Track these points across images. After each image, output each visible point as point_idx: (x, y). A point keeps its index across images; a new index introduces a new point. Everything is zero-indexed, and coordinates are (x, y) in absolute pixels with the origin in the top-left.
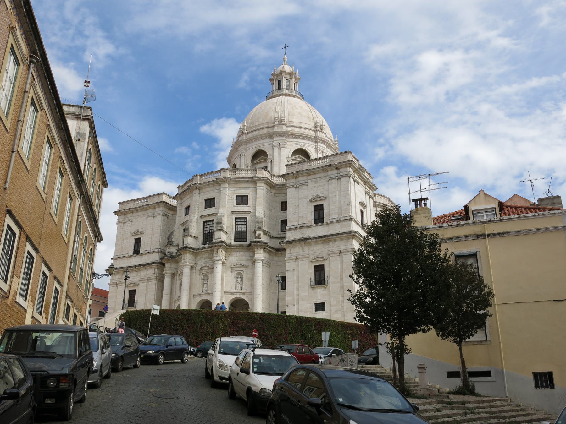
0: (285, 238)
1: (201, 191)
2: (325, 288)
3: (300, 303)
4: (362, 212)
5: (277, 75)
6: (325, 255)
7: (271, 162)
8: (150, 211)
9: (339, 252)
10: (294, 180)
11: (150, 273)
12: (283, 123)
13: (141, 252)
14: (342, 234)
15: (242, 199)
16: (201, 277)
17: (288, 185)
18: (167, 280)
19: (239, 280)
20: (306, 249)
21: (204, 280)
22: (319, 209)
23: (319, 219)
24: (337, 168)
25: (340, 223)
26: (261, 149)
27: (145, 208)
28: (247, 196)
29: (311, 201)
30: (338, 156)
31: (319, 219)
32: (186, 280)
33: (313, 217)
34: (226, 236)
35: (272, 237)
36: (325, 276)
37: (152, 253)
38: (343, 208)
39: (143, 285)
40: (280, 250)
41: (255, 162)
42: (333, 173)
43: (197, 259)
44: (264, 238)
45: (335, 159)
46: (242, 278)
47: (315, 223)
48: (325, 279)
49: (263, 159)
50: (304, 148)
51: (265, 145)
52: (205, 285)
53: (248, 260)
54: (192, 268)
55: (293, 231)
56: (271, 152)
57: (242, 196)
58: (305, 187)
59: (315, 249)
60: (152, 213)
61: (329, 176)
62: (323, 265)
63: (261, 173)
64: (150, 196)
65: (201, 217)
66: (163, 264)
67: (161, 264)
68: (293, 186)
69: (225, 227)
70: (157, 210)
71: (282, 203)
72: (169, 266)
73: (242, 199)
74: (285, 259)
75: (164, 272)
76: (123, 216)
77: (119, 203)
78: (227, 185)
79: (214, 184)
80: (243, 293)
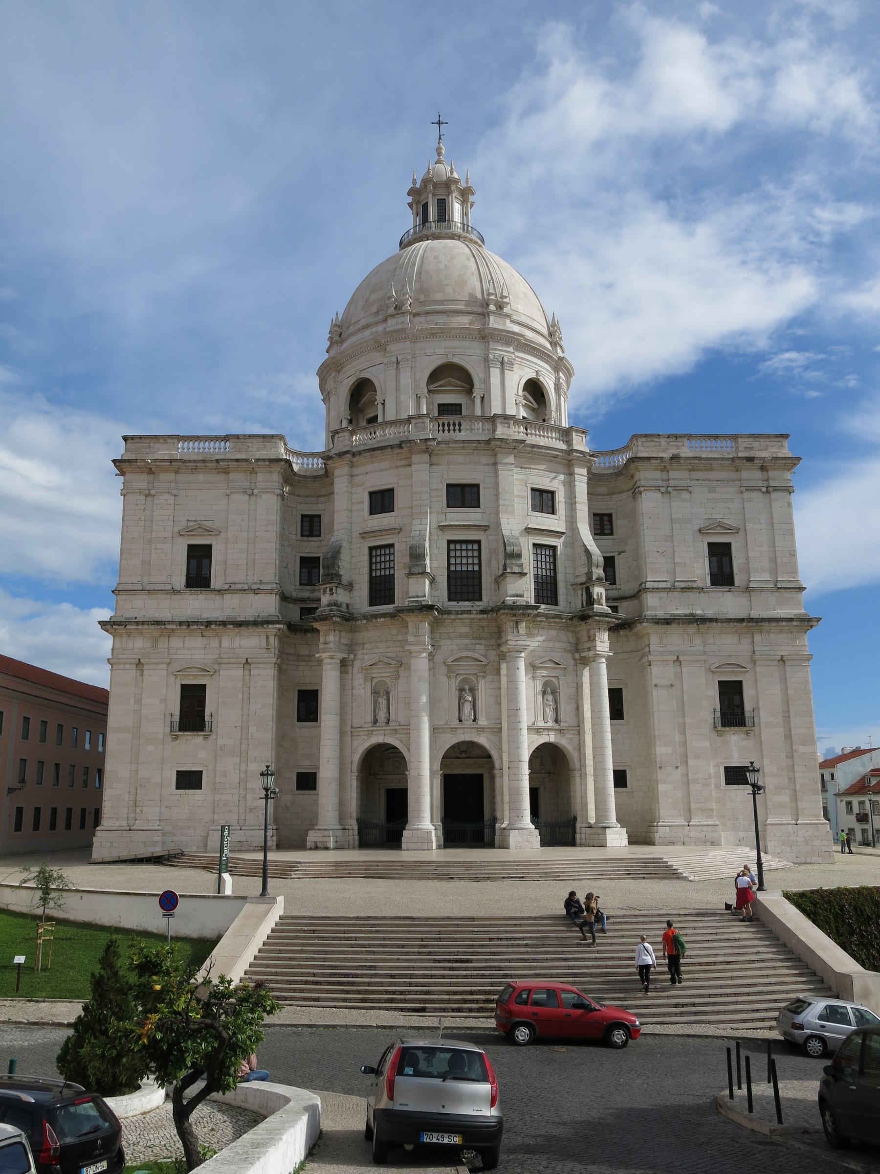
1: (434, 459)
3: (691, 762)
5: (435, 186)
7: (483, 398)
8: (238, 478)
9: (779, 658)
10: (658, 474)
12: (505, 310)
13: (216, 581)
14: (791, 620)
15: (544, 500)
16: (455, 684)
19: (550, 697)
20: (698, 640)
21: (461, 690)
23: (722, 574)
24: (763, 468)
25: (776, 594)
26: (456, 360)
27: (221, 466)
28: (552, 493)
30: (762, 440)
31: (722, 574)
33: (708, 571)
36: (748, 706)
37: (256, 592)
38: (779, 560)
41: (432, 387)
42: (752, 476)
43: (437, 636)
45: (756, 445)
46: (554, 692)
47: (713, 583)
48: (748, 714)
49: (450, 384)
50: (541, 379)
51: (468, 356)
52: (467, 708)
53: (566, 651)
55: (664, 595)
56: (482, 375)
57: (541, 492)
58: (685, 495)
60: (247, 484)
61: (745, 483)
62: (740, 682)
64: (237, 437)
68: (657, 488)
70: (260, 477)
72: (337, 639)
76: (145, 476)
77: (125, 438)
78: (511, 459)
79: (476, 449)
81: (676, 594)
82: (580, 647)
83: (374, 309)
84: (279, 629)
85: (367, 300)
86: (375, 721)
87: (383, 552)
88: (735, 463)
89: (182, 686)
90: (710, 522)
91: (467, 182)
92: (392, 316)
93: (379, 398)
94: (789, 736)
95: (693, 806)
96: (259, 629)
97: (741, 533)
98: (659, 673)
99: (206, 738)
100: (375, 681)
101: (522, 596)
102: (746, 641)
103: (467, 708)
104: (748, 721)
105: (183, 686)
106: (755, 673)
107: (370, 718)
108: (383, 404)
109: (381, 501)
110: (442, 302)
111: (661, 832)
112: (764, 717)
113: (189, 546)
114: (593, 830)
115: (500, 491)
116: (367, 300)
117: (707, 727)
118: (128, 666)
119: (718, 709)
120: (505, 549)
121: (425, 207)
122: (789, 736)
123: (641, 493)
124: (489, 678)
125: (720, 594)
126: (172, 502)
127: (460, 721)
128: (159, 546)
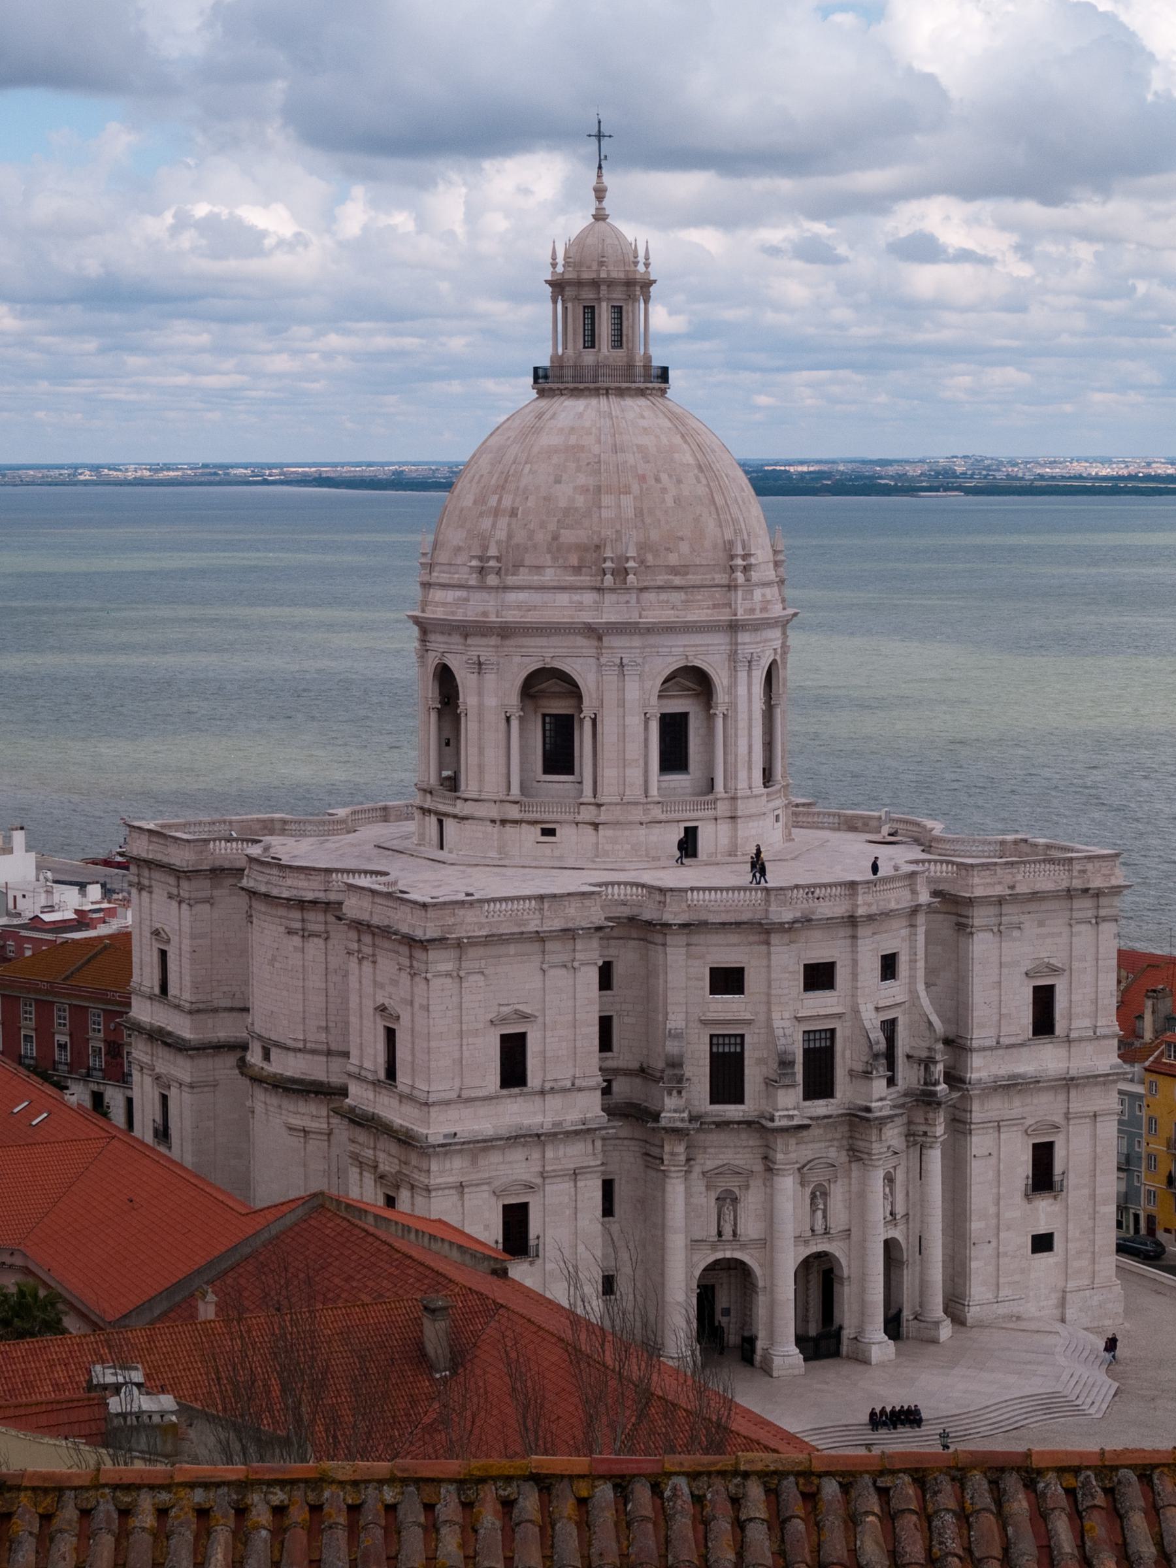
2: (1055, 1198)
6: (1058, 1119)
15: (889, 966)
16: (808, 1191)
21: (813, 1197)
22: (1044, 999)
23: (1043, 1023)
26: (697, 663)
33: (1031, 1020)
36: (1058, 1168)
37: (580, 1090)
39: (558, 1192)
42: (1084, 906)
47: (1034, 1034)
48: (1057, 1178)
55: (988, 1053)
56: (725, 682)
58: (1016, 933)
59: (1035, 1101)
64: (554, 896)
76: (453, 953)
81: (1000, 1052)
82: (913, 1127)
83: (574, 560)
85: (555, 538)
86: (720, 1234)
87: (727, 1041)
88: (1069, 894)
89: (504, 1206)
90: (1038, 962)
91: (647, 265)
92: (612, 590)
93: (587, 712)
94: (1093, 1196)
95: (1001, 1280)
96: (589, 1137)
97: (1067, 973)
98: (979, 1143)
99: (531, 1263)
100: (720, 1190)
102: (1062, 1097)
103: (819, 1214)
104: (1057, 1187)
105: (505, 1207)
106: (1068, 1132)
107: (714, 1232)
108: (594, 722)
109: (727, 980)
110: (673, 570)
111: (973, 1313)
112: (1072, 1181)
113: (502, 1036)
114: (922, 1325)
115: (859, 970)
116: (555, 538)
117: (1018, 1197)
118: (447, 1192)
120: (871, 1047)
121: (590, 312)
122: (1093, 1196)
123: (972, 933)
124: (839, 1182)
125: (1041, 1047)
126: (482, 984)
127: (813, 1231)
128: (471, 1040)
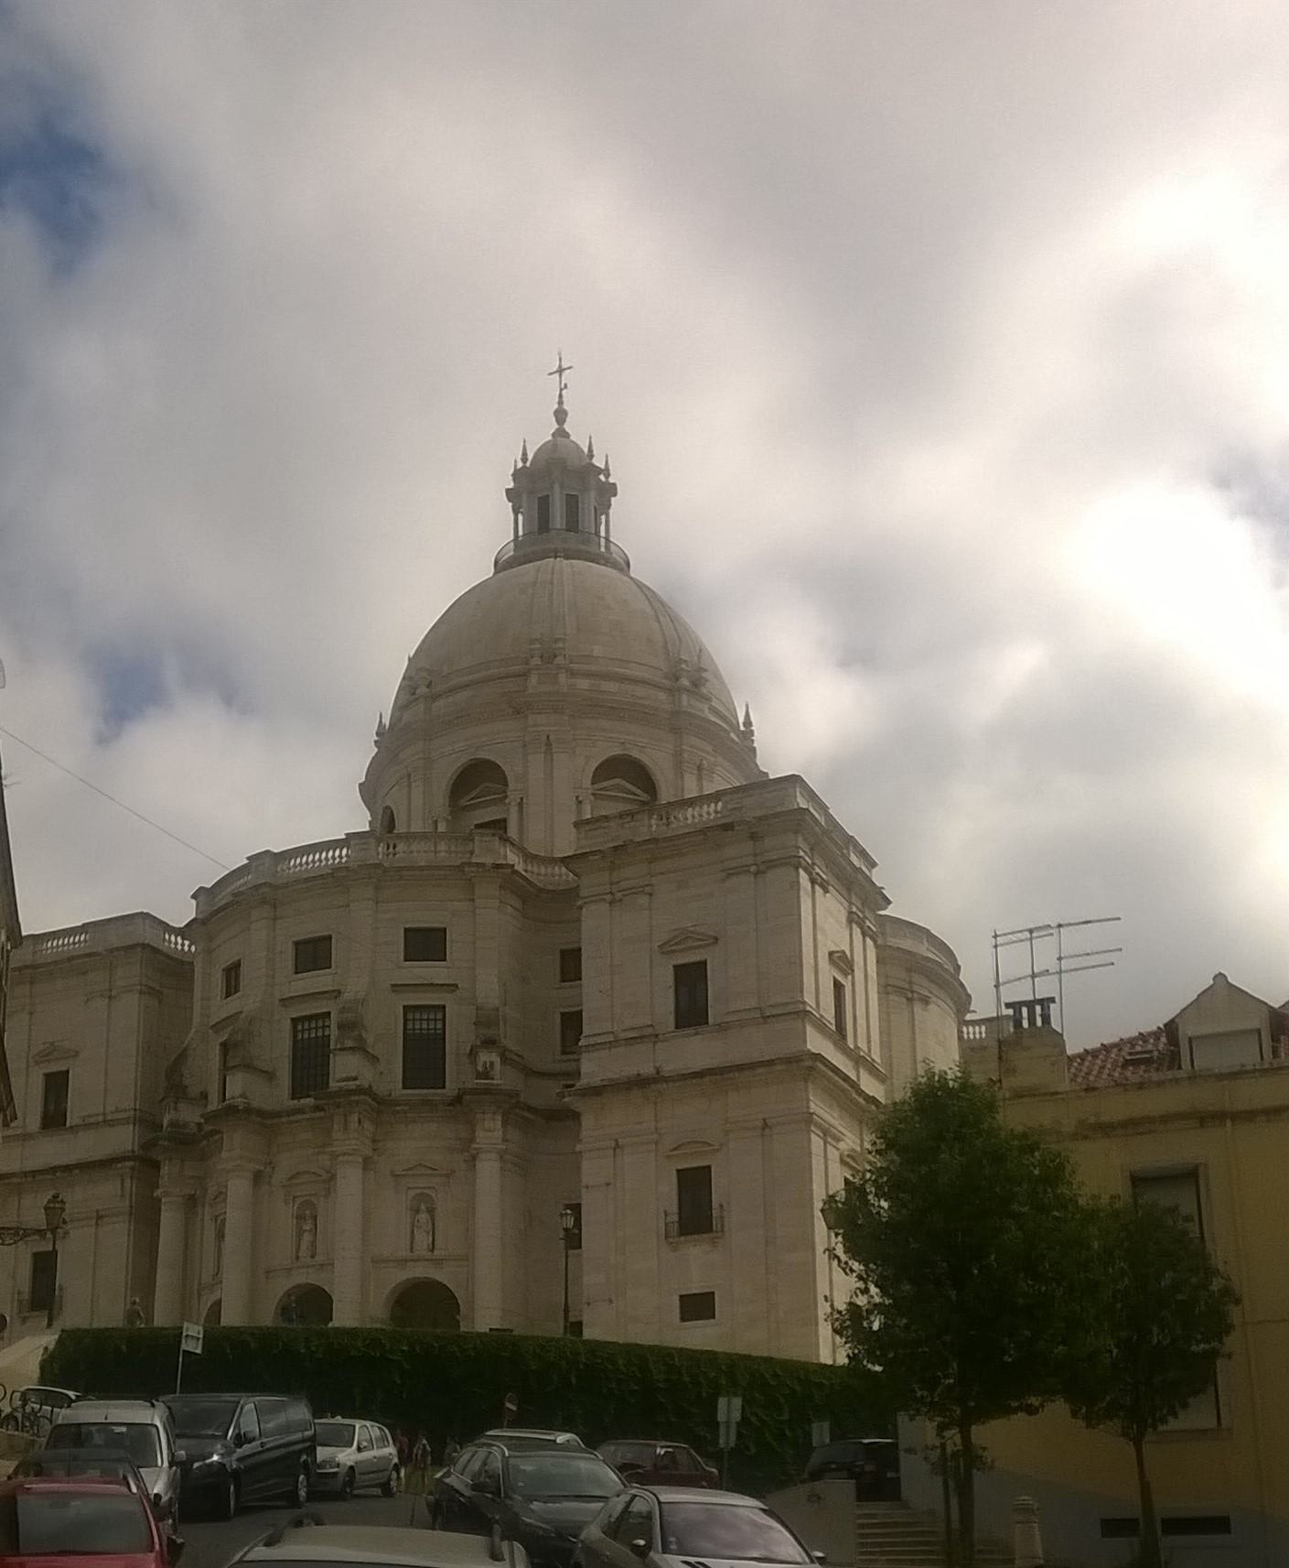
0: (577, 1074)
4: (838, 987)
7: (521, 805)
9: (760, 1123)
11: (109, 1192)
12: (559, 660)
17: (582, 893)
18: (169, 1221)
19: (423, 1217)
21: (300, 1217)
22: (691, 980)
23: (692, 1007)
24: (753, 837)
29: (666, 949)
31: (692, 1007)
32: (235, 1217)
33: (672, 1007)
34: (371, 1066)
35: (529, 1073)
40: (563, 1118)
41: (464, 802)
44: (503, 1078)
50: (635, 754)
52: (307, 1237)
54: (257, 1178)
58: (643, 900)
63: (488, 852)
65: (285, 1002)
66: (156, 1166)
67: (146, 1164)
69: (370, 1039)
71: (563, 953)
73: (426, 944)
74: (579, 1147)
75: (158, 1193)
80: (438, 1262)
84: (133, 1168)
101: (355, 1079)
113: (47, 1075)
119: (675, 1209)
